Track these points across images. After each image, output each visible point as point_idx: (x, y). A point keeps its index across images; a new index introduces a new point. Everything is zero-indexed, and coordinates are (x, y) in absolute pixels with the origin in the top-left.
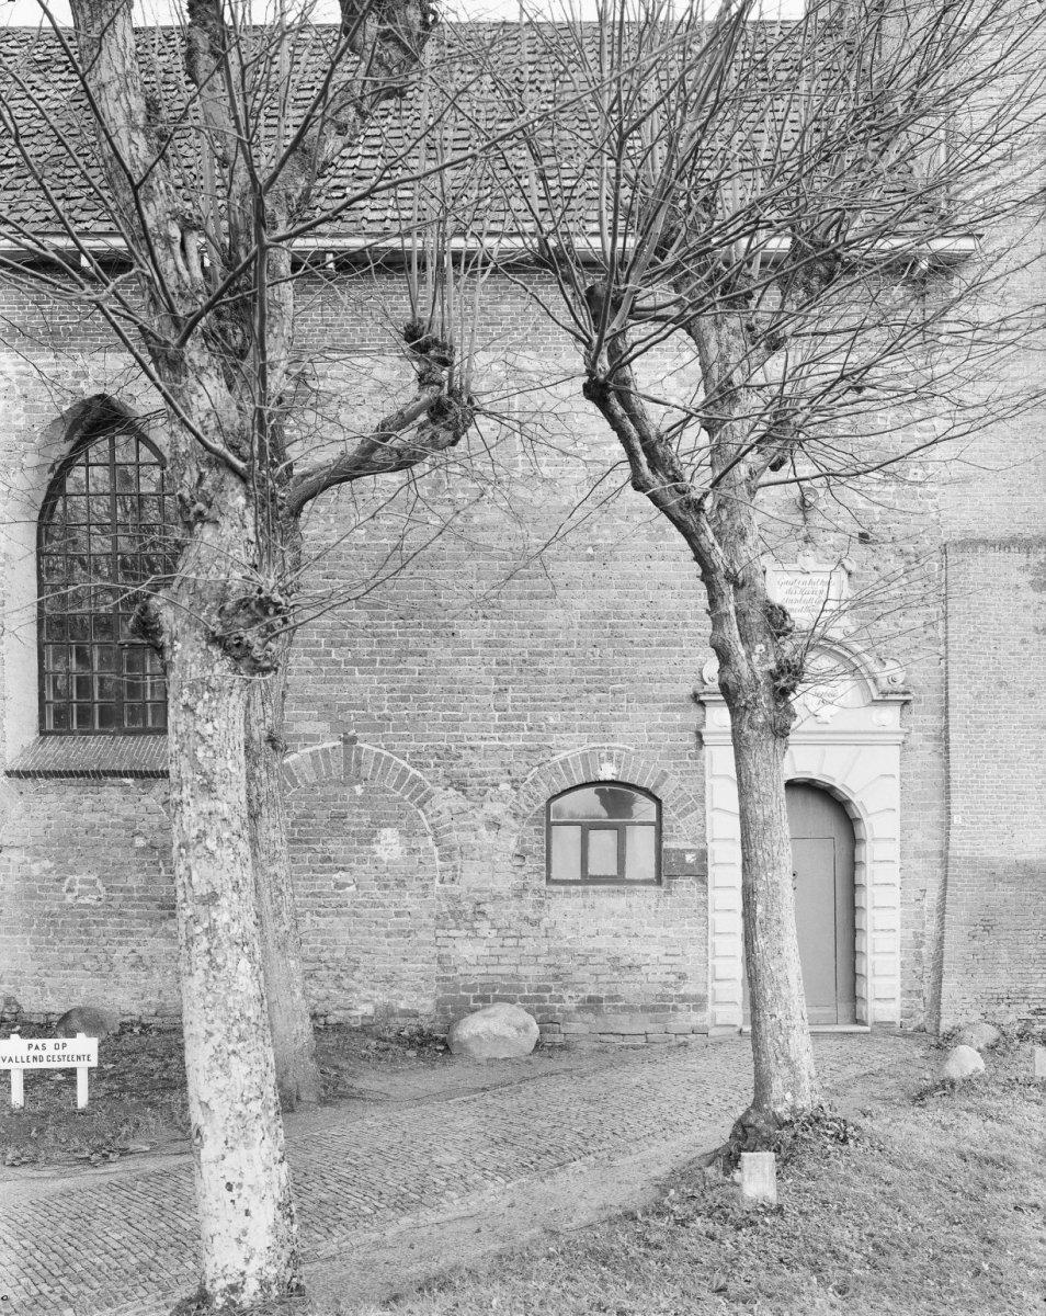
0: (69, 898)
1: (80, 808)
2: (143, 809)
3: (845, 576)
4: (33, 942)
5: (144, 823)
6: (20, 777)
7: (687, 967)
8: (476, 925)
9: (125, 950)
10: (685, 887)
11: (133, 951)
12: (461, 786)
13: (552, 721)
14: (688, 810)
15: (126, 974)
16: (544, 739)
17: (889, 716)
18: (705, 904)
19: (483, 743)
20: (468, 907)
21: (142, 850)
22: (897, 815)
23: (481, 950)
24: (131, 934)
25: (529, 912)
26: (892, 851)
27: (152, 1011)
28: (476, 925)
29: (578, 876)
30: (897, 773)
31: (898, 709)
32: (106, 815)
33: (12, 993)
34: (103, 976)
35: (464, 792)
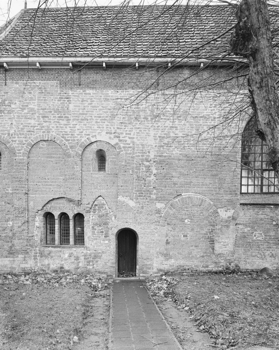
0: (255, 238)
1: (259, 214)
2: (275, 214)
4: (244, 250)
5: (275, 218)
6: (243, 205)
9: (269, 252)
11: (271, 253)
15: (269, 259)
21: (275, 225)
24: (270, 248)
27: (275, 269)
32: (265, 216)
33: (238, 264)
34: (263, 259)
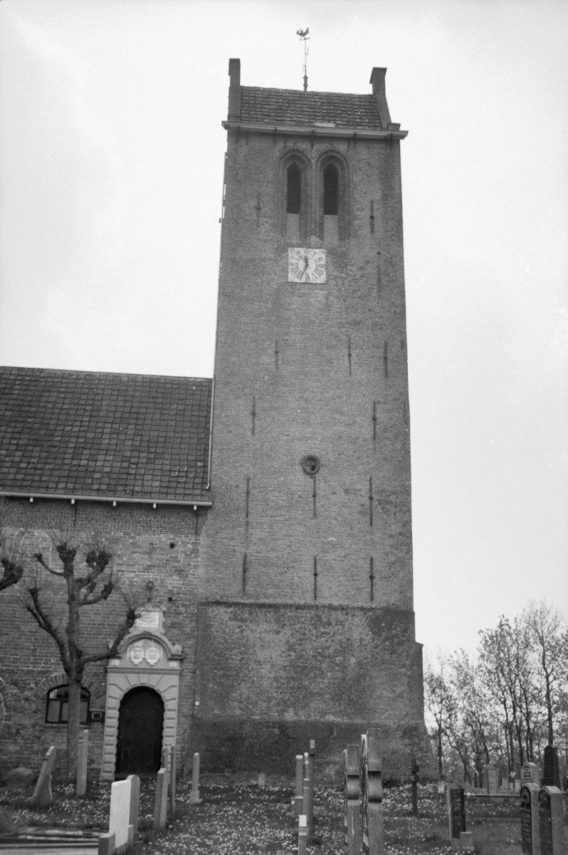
3: (162, 614)
7: (94, 757)
8: (16, 738)
10: (96, 725)
12: (15, 684)
13: (52, 661)
14: (99, 697)
16: (49, 668)
17: (175, 665)
18: (103, 733)
19: (26, 668)
20: (14, 730)
22: (177, 701)
23: (18, 748)
25: (37, 733)
26: (173, 714)
28: (16, 738)
29: (57, 720)
30: (178, 686)
31: (179, 662)
35: (18, 686)
